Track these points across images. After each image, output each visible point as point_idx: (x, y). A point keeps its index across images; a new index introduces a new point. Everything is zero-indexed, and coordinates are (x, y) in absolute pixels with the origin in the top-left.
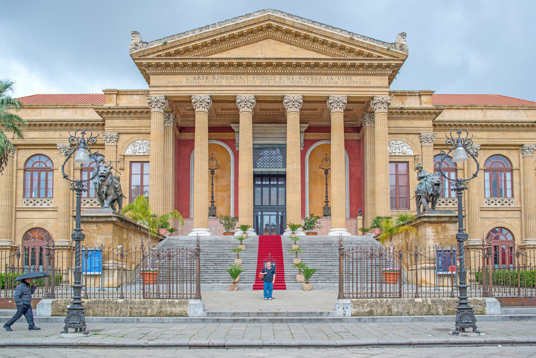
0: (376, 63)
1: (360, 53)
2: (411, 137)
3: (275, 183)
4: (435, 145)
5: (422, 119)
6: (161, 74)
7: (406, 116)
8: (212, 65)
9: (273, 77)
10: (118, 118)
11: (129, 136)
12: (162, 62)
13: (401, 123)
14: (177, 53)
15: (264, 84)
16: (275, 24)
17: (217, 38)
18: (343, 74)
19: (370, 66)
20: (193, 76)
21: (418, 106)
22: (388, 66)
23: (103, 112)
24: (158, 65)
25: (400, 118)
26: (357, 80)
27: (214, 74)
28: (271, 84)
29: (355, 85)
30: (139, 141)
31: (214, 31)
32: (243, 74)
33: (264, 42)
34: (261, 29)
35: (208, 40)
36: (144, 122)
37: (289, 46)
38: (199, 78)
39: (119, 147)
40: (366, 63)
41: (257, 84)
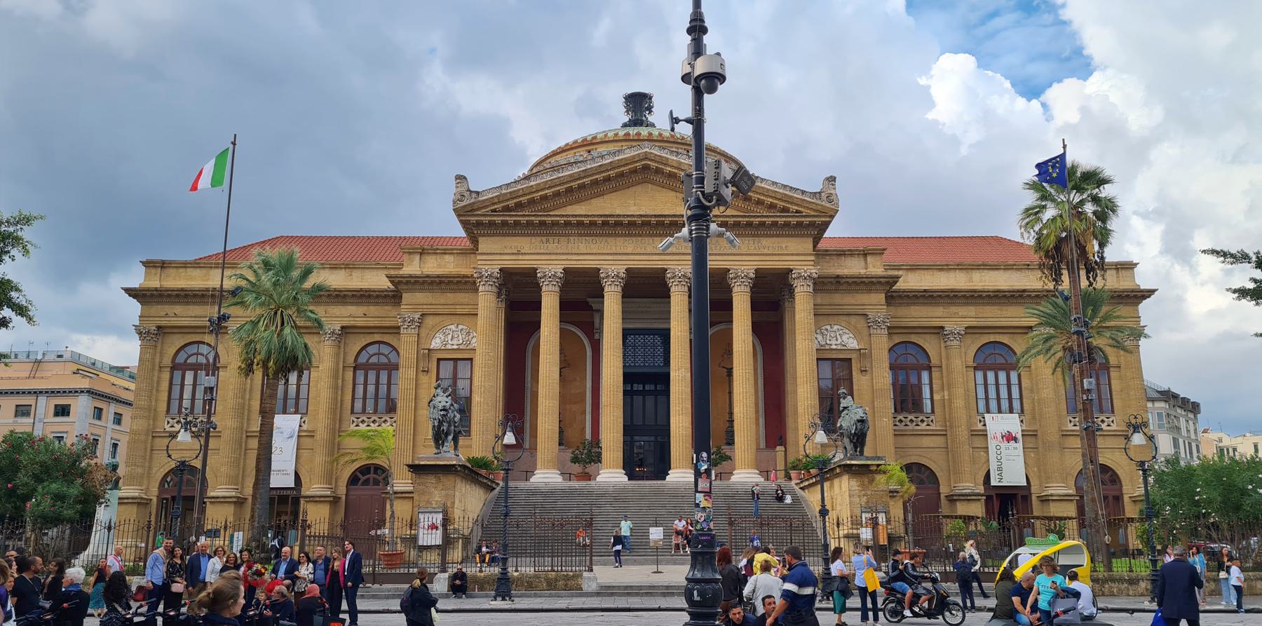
0: (794, 221)
1: (772, 206)
2: (853, 320)
3: (652, 387)
4: (889, 328)
5: (869, 291)
6: (494, 235)
7: (845, 287)
8: (567, 224)
9: (651, 240)
10: (421, 290)
11: (438, 319)
12: (498, 219)
13: (838, 298)
14: (519, 206)
15: (638, 251)
16: (654, 165)
17: (574, 184)
18: (748, 236)
19: (787, 225)
20: (539, 239)
21: (863, 272)
22: (812, 224)
23: (400, 282)
24: (492, 224)
25: (837, 291)
26: (769, 244)
27: (569, 235)
28: (649, 250)
29: (766, 251)
30: (453, 327)
31: (570, 176)
32: (610, 235)
33: (639, 188)
34: (634, 171)
35: (562, 188)
36: (462, 297)
37: (672, 194)
38: (548, 241)
39: (423, 335)
40: (781, 220)
41: (629, 250)
